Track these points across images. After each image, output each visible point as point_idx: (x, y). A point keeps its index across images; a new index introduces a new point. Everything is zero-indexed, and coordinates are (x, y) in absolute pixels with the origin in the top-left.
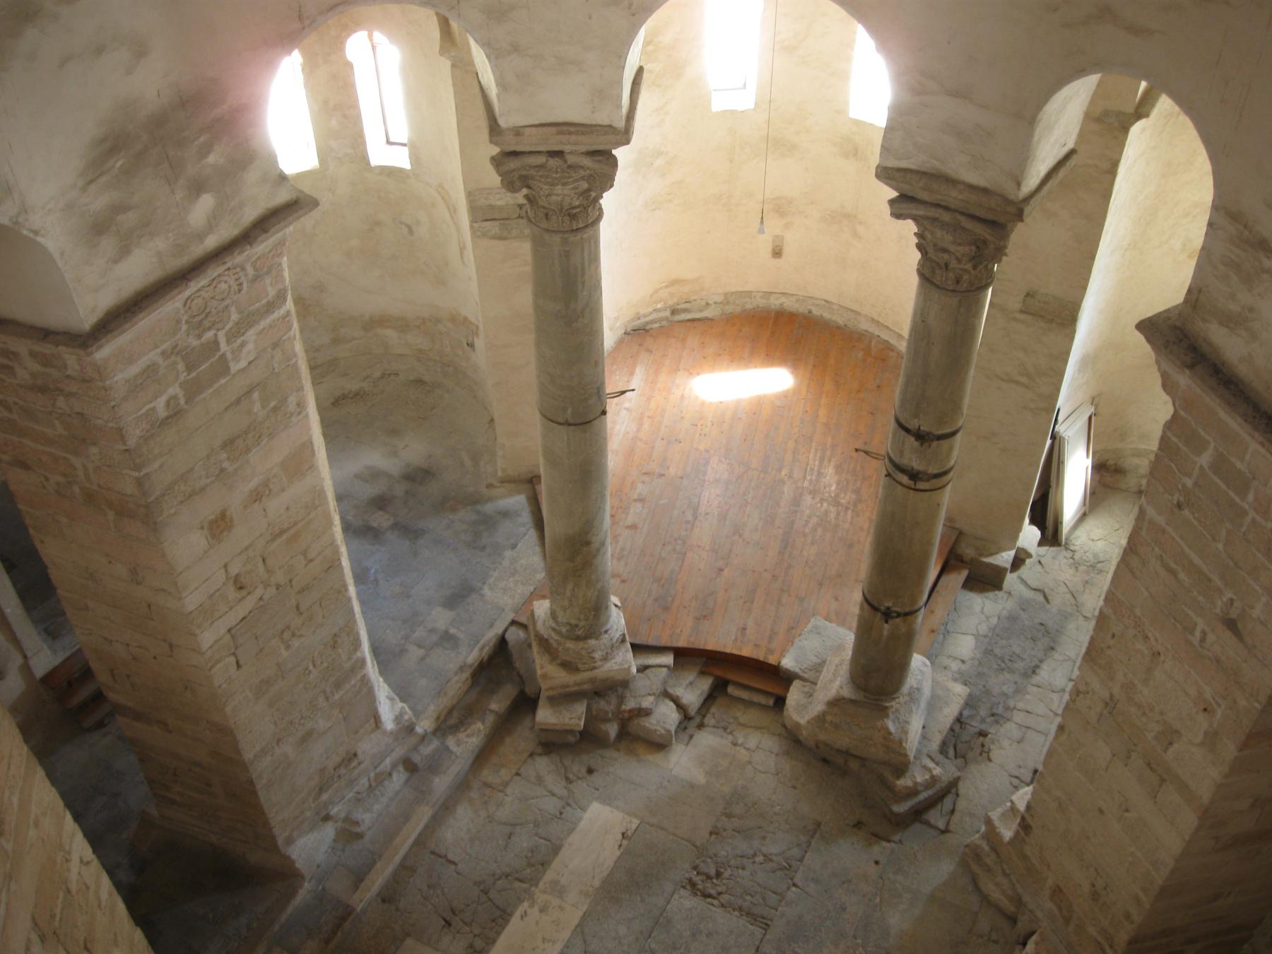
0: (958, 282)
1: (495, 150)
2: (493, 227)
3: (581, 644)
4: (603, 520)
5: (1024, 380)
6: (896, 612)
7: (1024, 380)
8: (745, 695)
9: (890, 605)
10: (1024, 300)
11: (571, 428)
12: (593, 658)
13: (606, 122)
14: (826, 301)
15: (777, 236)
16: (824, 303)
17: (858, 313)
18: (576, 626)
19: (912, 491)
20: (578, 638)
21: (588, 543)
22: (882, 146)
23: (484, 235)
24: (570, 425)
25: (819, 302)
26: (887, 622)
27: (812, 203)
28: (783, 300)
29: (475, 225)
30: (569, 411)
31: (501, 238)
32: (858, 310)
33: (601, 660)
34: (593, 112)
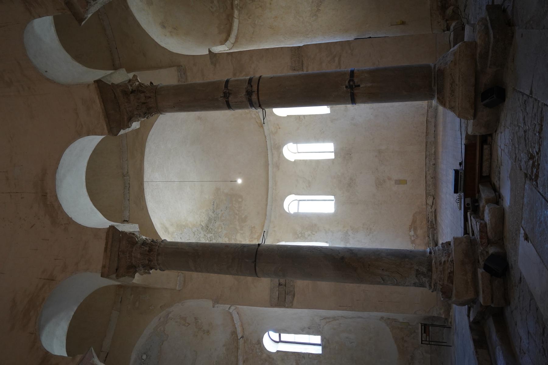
0: (150, 97)
1: (114, 276)
2: (289, 298)
3: (434, 269)
4: (332, 249)
5: (337, 59)
6: (349, 82)
7: (337, 59)
8: (486, 164)
9: (344, 87)
10: (297, 71)
11: (257, 260)
12: (445, 262)
13: (105, 234)
14: (426, 159)
15: (395, 183)
16: (427, 159)
17: (427, 142)
18: (417, 270)
19: (259, 92)
20: (430, 270)
21: (343, 258)
22: (101, 135)
23: (292, 302)
24: (255, 261)
25: (428, 161)
26: (359, 86)
27: (377, 169)
28: (429, 177)
29: (286, 306)
30: (247, 261)
31: (294, 295)
32: (425, 143)
33: (449, 257)
34: (101, 239)
